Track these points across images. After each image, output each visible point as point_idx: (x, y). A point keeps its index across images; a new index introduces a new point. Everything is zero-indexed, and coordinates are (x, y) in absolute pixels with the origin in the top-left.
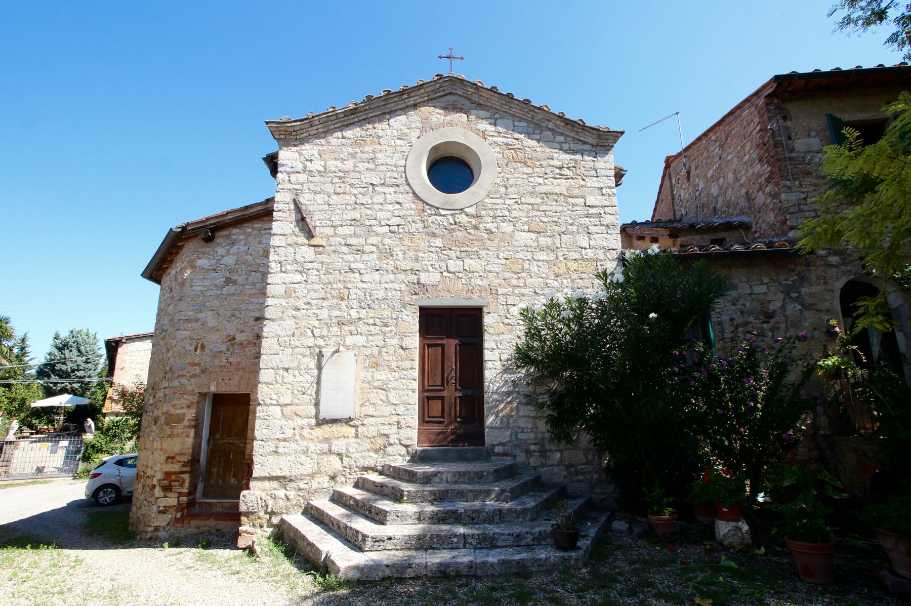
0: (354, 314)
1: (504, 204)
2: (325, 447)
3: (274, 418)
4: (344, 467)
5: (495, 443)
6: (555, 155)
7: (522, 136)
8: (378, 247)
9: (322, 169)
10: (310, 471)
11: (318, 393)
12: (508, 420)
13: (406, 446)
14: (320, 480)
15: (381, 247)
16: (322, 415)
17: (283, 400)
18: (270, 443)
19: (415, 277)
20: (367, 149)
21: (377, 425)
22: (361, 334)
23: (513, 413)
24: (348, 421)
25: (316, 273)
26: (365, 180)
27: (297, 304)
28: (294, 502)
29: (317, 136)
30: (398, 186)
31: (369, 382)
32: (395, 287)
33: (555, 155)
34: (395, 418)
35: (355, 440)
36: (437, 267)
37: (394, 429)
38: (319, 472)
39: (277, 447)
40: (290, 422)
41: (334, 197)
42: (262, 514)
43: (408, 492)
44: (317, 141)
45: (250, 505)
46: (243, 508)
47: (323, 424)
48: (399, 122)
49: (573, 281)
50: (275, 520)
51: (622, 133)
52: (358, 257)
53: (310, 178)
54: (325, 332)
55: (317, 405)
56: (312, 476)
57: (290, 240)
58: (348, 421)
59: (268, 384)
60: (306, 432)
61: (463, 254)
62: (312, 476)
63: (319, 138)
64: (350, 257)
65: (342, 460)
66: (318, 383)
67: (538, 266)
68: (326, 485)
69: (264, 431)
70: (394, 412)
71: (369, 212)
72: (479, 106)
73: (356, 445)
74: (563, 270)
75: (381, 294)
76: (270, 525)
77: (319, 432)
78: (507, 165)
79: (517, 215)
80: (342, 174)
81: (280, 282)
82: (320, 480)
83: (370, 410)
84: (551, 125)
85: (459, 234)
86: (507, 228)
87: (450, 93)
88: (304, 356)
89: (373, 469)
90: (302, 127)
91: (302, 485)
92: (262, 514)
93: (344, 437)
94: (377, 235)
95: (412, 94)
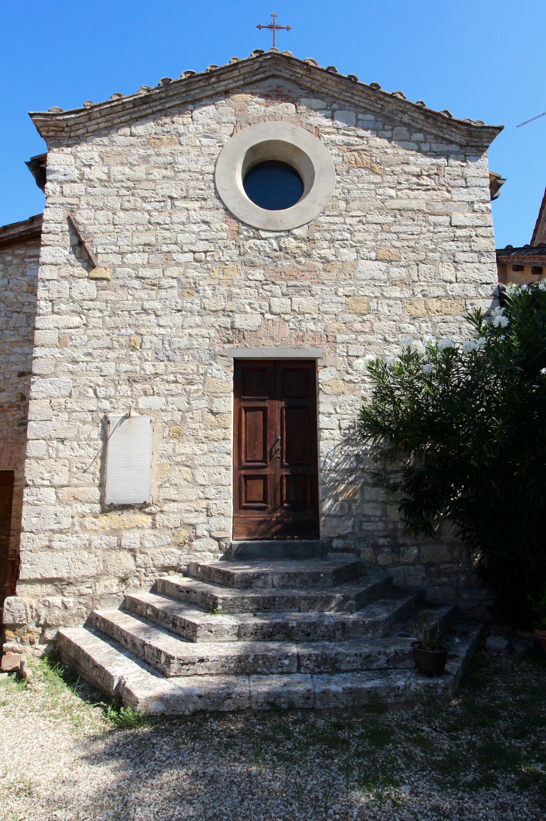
0: (149, 368)
1: (345, 223)
2: (114, 540)
3: (47, 503)
4: (138, 566)
5: (332, 535)
6: (412, 158)
7: (368, 134)
8: (179, 280)
9: (105, 177)
10: (93, 572)
11: (103, 470)
12: (350, 506)
13: (218, 540)
14: (107, 583)
15: (183, 280)
16: (109, 500)
17: (57, 481)
18: (41, 535)
19: (229, 320)
20: (163, 150)
21: (180, 512)
22: (158, 394)
23: (357, 497)
24: (142, 507)
25: (99, 314)
26: (161, 192)
27: (75, 355)
28: (74, 612)
29: (97, 133)
30: (205, 200)
31: (169, 457)
32: (203, 332)
33: (412, 158)
34: (204, 504)
35: (152, 532)
36: (256, 306)
37: (202, 518)
38: (106, 573)
39: (50, 541)
40: (68, 508)
41: (121, 214)
42: (32, 627)
43: (224, 599)
44: (98, 140)
45: (17, 615)
46: (8, 619)
47: (110, 511)
48: (205, 114)
49: (434, 325)
50: (50, 635)
51: (500, 129)
52: (153, 293)
53: (90, 190)
54: (111, 391)
55: (102, 486)
56: (97, 578)
57: (66, 271)
58: (142, 507)
59: (37, 459)
60: (88, 521)
61: (291, 290)
62: (97, 578)
63: (99, 136)
64: (143, 294)
65: (135, 557)
66: (104, 458)
67: (389, 306)
68: (115, 589)
69: (34, 520)
70: (202, 495)
71: (167, 234)
72: (312, 93)
73: (153, 538)
74: (421, 310)
75: (184, 342)
76: (43, 640)
77: (105, 521)
78: (348, 172)
79: (361, 239)
80: (131, 184)
81: (51, 326)
82: (107, 583)
83: (172, 493)
84: (406, 119)
85: (286, 263)
86: (348, 255)
87: (273, 76)
88: (84, 423)
89: (176, 569)
90: (78, 121)
91: (84, 589)
92: (32, 627)
93: (138, 527)
94: (178, 264)
95: (223, 77)
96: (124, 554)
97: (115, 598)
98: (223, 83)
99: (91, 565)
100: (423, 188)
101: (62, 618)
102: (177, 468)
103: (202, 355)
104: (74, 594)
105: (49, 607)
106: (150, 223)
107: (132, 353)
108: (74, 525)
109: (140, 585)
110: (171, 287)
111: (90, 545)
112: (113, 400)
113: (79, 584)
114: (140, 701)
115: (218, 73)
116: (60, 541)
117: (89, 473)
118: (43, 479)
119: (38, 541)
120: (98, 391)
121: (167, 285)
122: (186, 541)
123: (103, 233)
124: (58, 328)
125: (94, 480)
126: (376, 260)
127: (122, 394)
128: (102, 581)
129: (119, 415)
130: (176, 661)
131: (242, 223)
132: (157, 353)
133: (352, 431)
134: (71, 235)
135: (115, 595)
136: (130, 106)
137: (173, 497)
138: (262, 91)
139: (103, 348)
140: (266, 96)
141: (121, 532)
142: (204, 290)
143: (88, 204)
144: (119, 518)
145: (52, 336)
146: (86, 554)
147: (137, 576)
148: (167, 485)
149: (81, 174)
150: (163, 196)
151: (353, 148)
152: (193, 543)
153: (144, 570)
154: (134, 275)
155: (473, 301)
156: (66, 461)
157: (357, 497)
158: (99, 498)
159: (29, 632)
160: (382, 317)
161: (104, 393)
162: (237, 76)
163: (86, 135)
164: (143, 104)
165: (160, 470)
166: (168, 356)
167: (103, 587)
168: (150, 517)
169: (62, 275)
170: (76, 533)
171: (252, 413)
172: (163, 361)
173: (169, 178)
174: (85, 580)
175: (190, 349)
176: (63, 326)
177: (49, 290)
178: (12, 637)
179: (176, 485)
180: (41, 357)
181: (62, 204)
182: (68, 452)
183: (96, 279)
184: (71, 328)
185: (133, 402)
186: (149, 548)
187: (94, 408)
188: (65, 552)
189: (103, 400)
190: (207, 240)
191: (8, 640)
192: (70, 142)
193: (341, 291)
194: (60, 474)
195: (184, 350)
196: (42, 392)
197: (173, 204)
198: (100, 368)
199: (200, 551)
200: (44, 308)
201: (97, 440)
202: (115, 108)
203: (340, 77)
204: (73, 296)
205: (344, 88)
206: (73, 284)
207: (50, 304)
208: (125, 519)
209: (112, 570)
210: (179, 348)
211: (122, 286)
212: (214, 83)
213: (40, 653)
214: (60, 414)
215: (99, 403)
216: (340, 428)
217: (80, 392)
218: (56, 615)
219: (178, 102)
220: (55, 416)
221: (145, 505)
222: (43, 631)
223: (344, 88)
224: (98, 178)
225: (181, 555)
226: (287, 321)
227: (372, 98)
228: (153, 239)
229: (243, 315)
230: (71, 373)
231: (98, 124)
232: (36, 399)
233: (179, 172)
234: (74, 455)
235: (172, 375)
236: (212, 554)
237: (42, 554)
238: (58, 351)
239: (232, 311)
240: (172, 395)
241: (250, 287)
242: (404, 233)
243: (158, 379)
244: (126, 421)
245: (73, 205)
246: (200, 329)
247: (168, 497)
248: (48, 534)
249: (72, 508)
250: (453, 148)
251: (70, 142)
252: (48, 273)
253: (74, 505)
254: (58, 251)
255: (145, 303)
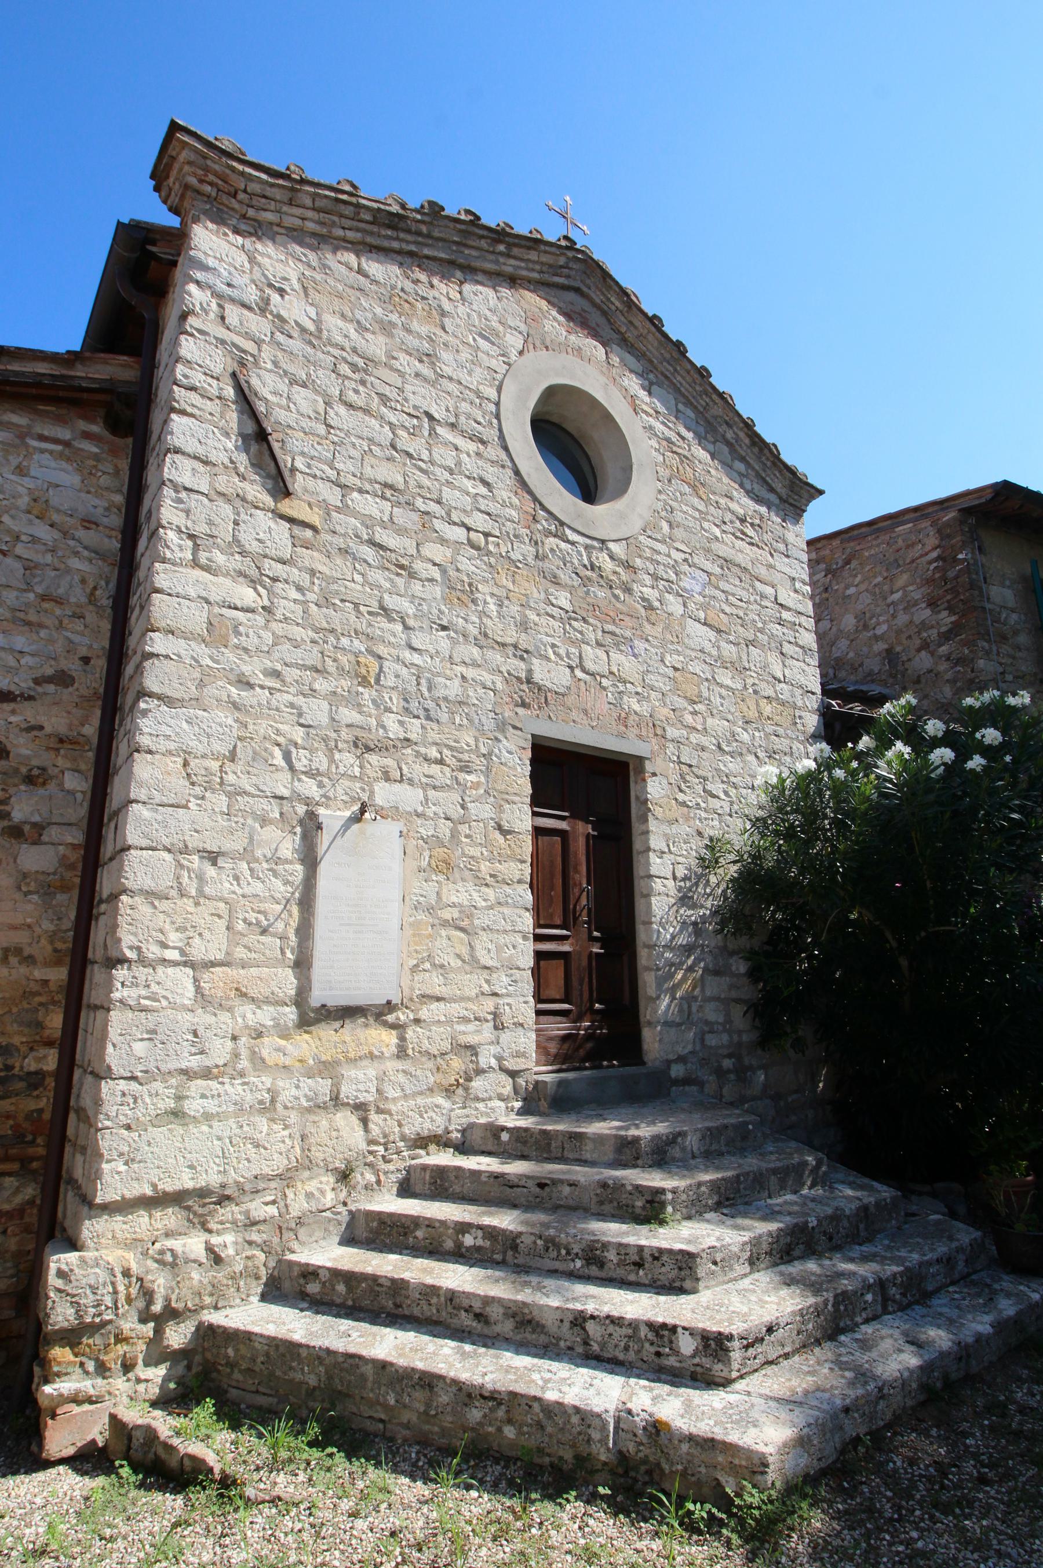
0: (394, 730)
1: (669, 556)
2: (323, 1087)
3: (173, 1006)
4: (371, 1142)
5: (671, 1057)
6: (735, 493)
7: (690, 435)
8: (444, 571)
9: (311, 327)
10: (278, 1163)
11: (305, 930)
12: (690, 1007)
13: (513, 1074)
14: (312, 1186)
15: (452, 573)
16: (318, 996)
17: (199, 950)
18: (158, 1086)
19: (523, 665)
20: (415, 326)
21: (449, 1022)
22: (411, 782)
23: (697, 992)
24: (380, 1013)
25: (294, 594)
26: (413, 400)
27: (246, 669)
28: (238, 1268)
29: (297, 235)
30: (483, 442)
31: (430, 910)
32: (475, 677)
33: (735, 493)
34: (489, 1004)
35: (400, 1065)
36: (562, 652)
37: (487, 1031)
38: (307, 1164)
39: (179, 1098)
40: (224, 1017)
41: (342, 410)
42: (129, 1324)
43: (674, 1191)
44: (298, 249)
45: (88, 1300)
46: (61, 1315)
47: (317, 1021)
48: (483, 298)
49: (767, 735)
50: (177, 1336)
51: (821, 492)
52: (400, 582)
53: (280, 337)
54: (321, 762)
55: (302, 964)
56: (286, 1178)
57: (227, 482)
58: (380, 1013)
59: (151, 895)
60: (267, 1047)
61: (609, 639)
62: (286, 1178)
63: (301, 244)
64: (377, 576)
65: (365, 1121)
66: (307, 901)
67: (722, 697)
68: (329, 1199)
69: (139, 1048)
70: (486, 988)
71: (425, 481)
72: (625, 343)
73: (401, 1078)
74: (752, 714)
75: (453, 689)
76: (157, 1352)
77: (305, 1045)
78: (670, 481)
79: (688, 587)
80: (360, 362)
81: (193, 594)
82: (312, 1186)
83: (434, 983)
84: (729, 435)
85: (601, 594)
86: (675, 606)
87: (577, 290)
88: (264, 821)
89: (441, 1141)
90: (269, 192)
91: (260, 1208)
92: (129, 1324)
93: (372, 1056)
94: (443, 541)
95: (516, 251)
96: (345, 1118)
97: (330, 1220)
98: (512, 262)
99: (278, 1149)
100: (748, 540)
101: (210, 1288)
102: (443, 933)
103: (484, 719)
104: (234, 1222)
105: (174, 1265)
106: (393, 446)
107: (361, 689)
108: (236, 1055)
109: (379, 1182)
110: (431, 580)
111: (273, 1101)
112: (325, 780)
113: (247, 1199)
114: (771, 1459)
115: (511, 240)
116: (203, 1096)
117: (274, 935)
118: (164, 946)
119: (148, 1100)
120: (294, 755)
121: (424, 575)
122: (461, 1081)
123: (305, 433)
124: (208, 602)
125: (283, 953)
126: (705, 624)
127: (342, 770)
128: (299, 1184)
129: (338, 813)
130: (736, 1344)
131: (541, 504)
132: (406, 700)
133: (688, 884)
134: (241, 412)
135: (328, 1214)
136: (368, 217)
137: (438, 991)
138: (562, 305)
139: (305, 667)
140: (568, 316)
141: (339, 1069)
142: (485, 602)
143: (275, 363)
144: (335, 1037)
145: (195, 617)
146: (263, 1123)
147: (369, 1165)
148: (427, 965)
149: (262, 299)
150: (415, 407)
151: (675, 449)
152: (473, 1084)
153: (381, 1148)
154: (366, 537)
155: (803, 714)
156: (222, 905)
157: (697, 992)
158: (293, 992)
159: (120, 1339)
160: (715, 711)
161: (305, 762)
162: (534, 262)
163: (276, 228)
164: (389, 227)
165: (414, 935)
166: (426, 710)
167: (302, 1197)
168: (394, 1032)
169: (220, 489)
170: (242, 1075)
171: (546, 838)
172: (418, 717)
173: (425, 380)
174: (261, 1185)
175: (464, 703)
176: (218, 598)
177: (188, 512)
178: (70, 1363)
179: (442, 966)
180: (167, 657)
181: (223, 342)
182: (227, 886)
183: (291, 520)
184: (236, 608)
185: (363, 790)
186: (394, 1099)
187: (286, 793)
188: (215, 1124)
189: (303, 777)
190: (489, 514)
191: (58, 1375)
192: (243, 227)
193: (668, 659)
194: (207, 934)
195: (454, 703)
196: (168, 737)
197: (432, 429)
198: (299, 708)
199: (483, 1100)
200: (176, 549)
201: (291, 863)
202: (342, 207)
203: (666, 336)
204: (243, 542)
205: (667, 356)
206: (243, 516)
207: (190, 543)
208: (348, 1039)
209: (321, 1156)
210: (446, 699)
211: (344, 551)
212: (501, 254)
213: (154, 1391)
214: (208, 794)
215: (296, 783)
216: (675, 878)
217: (255, 752)
218: (195, 1282)
219: (443, 255)
220: (196, 797)
221: (390, 1006)
222: (158, 1332)
223: (667, 356)
224: (296, 322)
225: (452, 1110)
226: (604, 689)
227: (698, 388)
228: (401, 480)
229: (544, 663)
230: (236, 706)
231: (303, 219)
232: (150, 752)
233: (442, 376)
234: (239, 891)
235: (434, 748)
236: (502, 1104)
237: (157, 1133)
238: (207, 650)
239: (527, 651)
240: (434, 788)
241: (553, 617)
242: (733, 595)
243: (409, 751)
244: (356, 827)
245: (244, 351)
246: (479, 671)
247: (429, 992)
248: (173, 1081)
249: (233, 1017)
250: (772, 497)
251: (243, 227)
252: (189, 474)
253: (239, 1011)
254: (211, 435)
255: (386, 596)
